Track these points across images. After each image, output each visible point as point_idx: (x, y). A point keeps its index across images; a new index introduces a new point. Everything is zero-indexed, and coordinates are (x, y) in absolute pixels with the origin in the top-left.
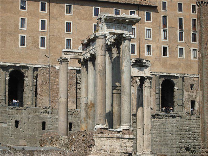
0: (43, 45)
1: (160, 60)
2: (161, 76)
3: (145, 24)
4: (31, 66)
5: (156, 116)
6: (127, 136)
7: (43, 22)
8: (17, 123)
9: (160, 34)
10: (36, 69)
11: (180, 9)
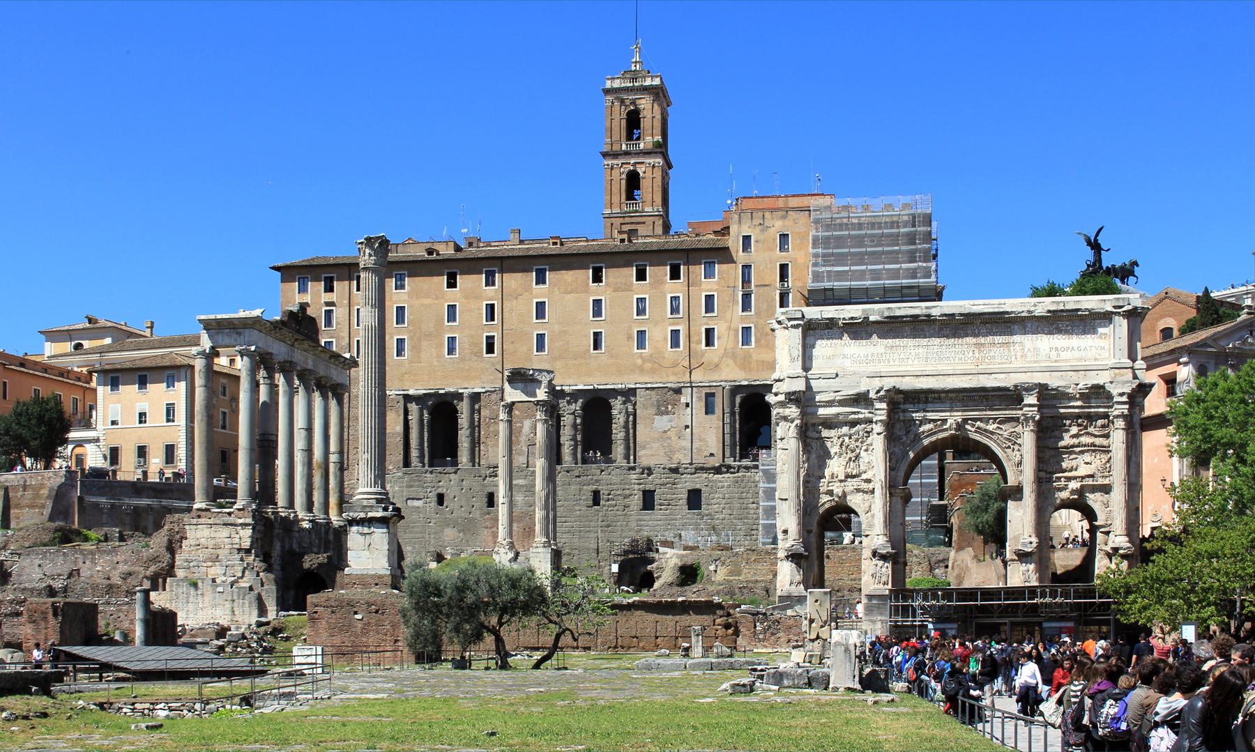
0: (490, 349)
1: (734, 356)
2: (736, 390)
3: (703, 287)
4: (466, 392)
5: (724, 470)
6: (240, 521)
7: (491, 308)
8: (441, 499)
9: (734, 301)
10: (475, 398)
11: (783, 248)
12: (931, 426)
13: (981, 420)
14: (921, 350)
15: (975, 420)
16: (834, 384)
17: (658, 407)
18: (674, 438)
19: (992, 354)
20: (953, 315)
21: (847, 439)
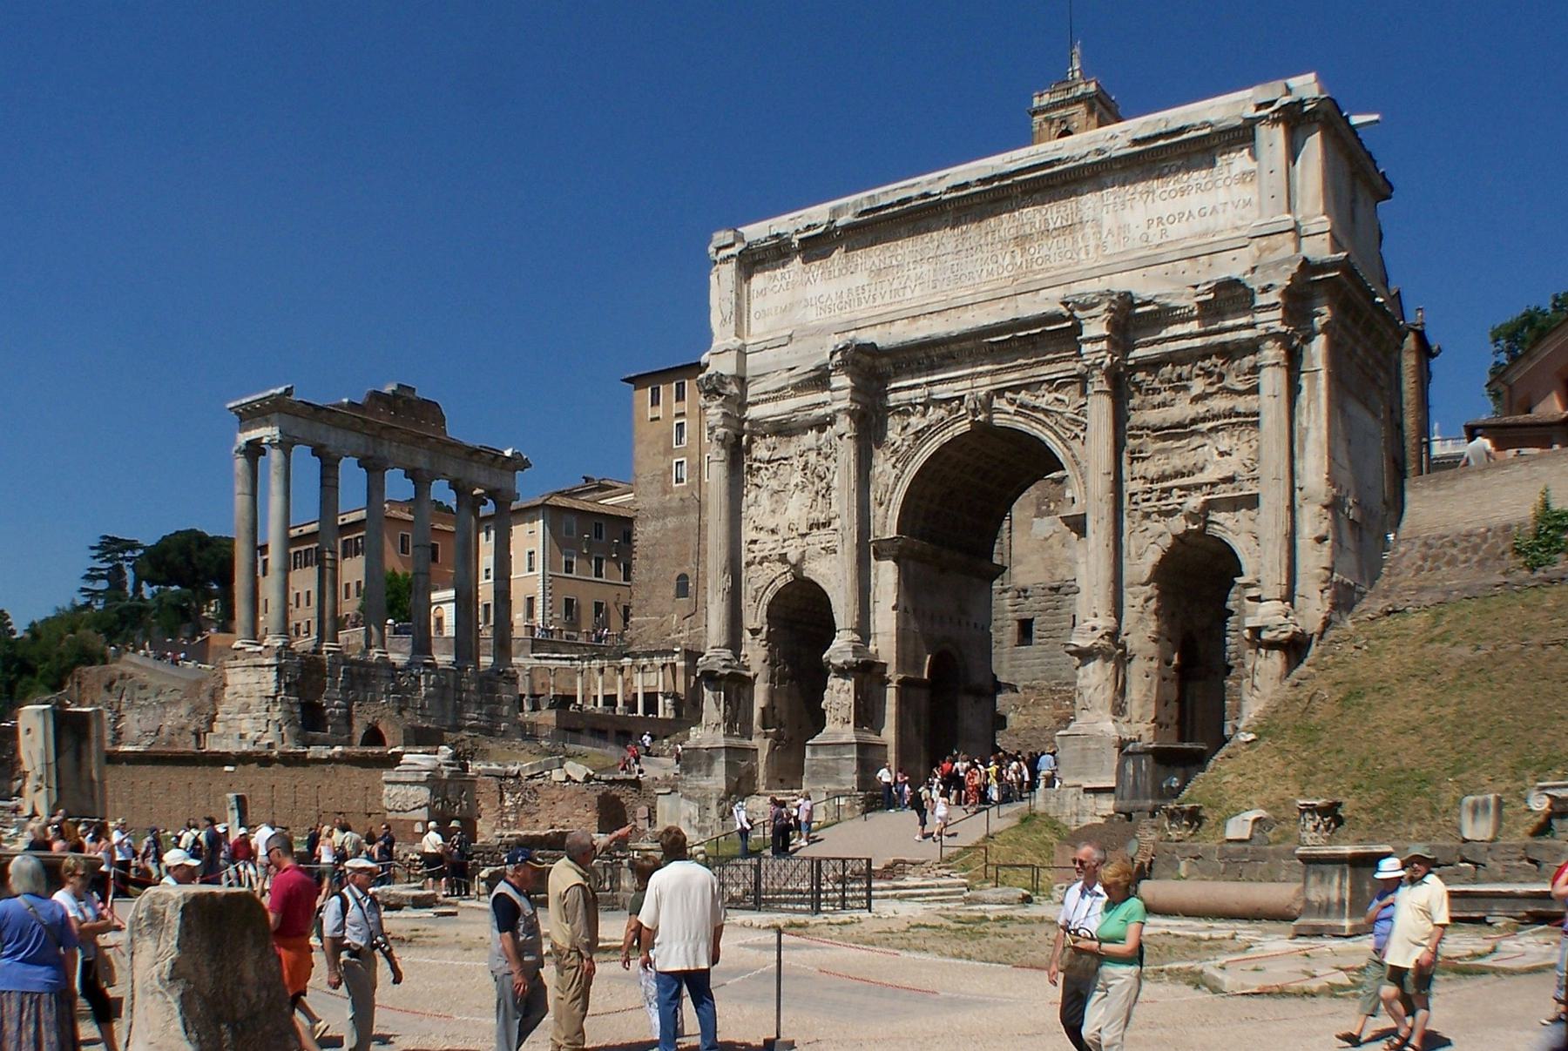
12: (942, 412)
13: (1027, 387)
14: (926, 267)
15: (1016, 389)
16: (786, 356)
17: (1038, 508)
18: (1057, 547)
19: (1044, 252)
20: (966, 185)
21: (812, 457)
